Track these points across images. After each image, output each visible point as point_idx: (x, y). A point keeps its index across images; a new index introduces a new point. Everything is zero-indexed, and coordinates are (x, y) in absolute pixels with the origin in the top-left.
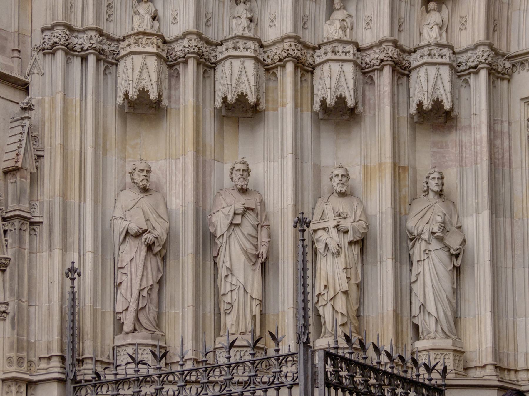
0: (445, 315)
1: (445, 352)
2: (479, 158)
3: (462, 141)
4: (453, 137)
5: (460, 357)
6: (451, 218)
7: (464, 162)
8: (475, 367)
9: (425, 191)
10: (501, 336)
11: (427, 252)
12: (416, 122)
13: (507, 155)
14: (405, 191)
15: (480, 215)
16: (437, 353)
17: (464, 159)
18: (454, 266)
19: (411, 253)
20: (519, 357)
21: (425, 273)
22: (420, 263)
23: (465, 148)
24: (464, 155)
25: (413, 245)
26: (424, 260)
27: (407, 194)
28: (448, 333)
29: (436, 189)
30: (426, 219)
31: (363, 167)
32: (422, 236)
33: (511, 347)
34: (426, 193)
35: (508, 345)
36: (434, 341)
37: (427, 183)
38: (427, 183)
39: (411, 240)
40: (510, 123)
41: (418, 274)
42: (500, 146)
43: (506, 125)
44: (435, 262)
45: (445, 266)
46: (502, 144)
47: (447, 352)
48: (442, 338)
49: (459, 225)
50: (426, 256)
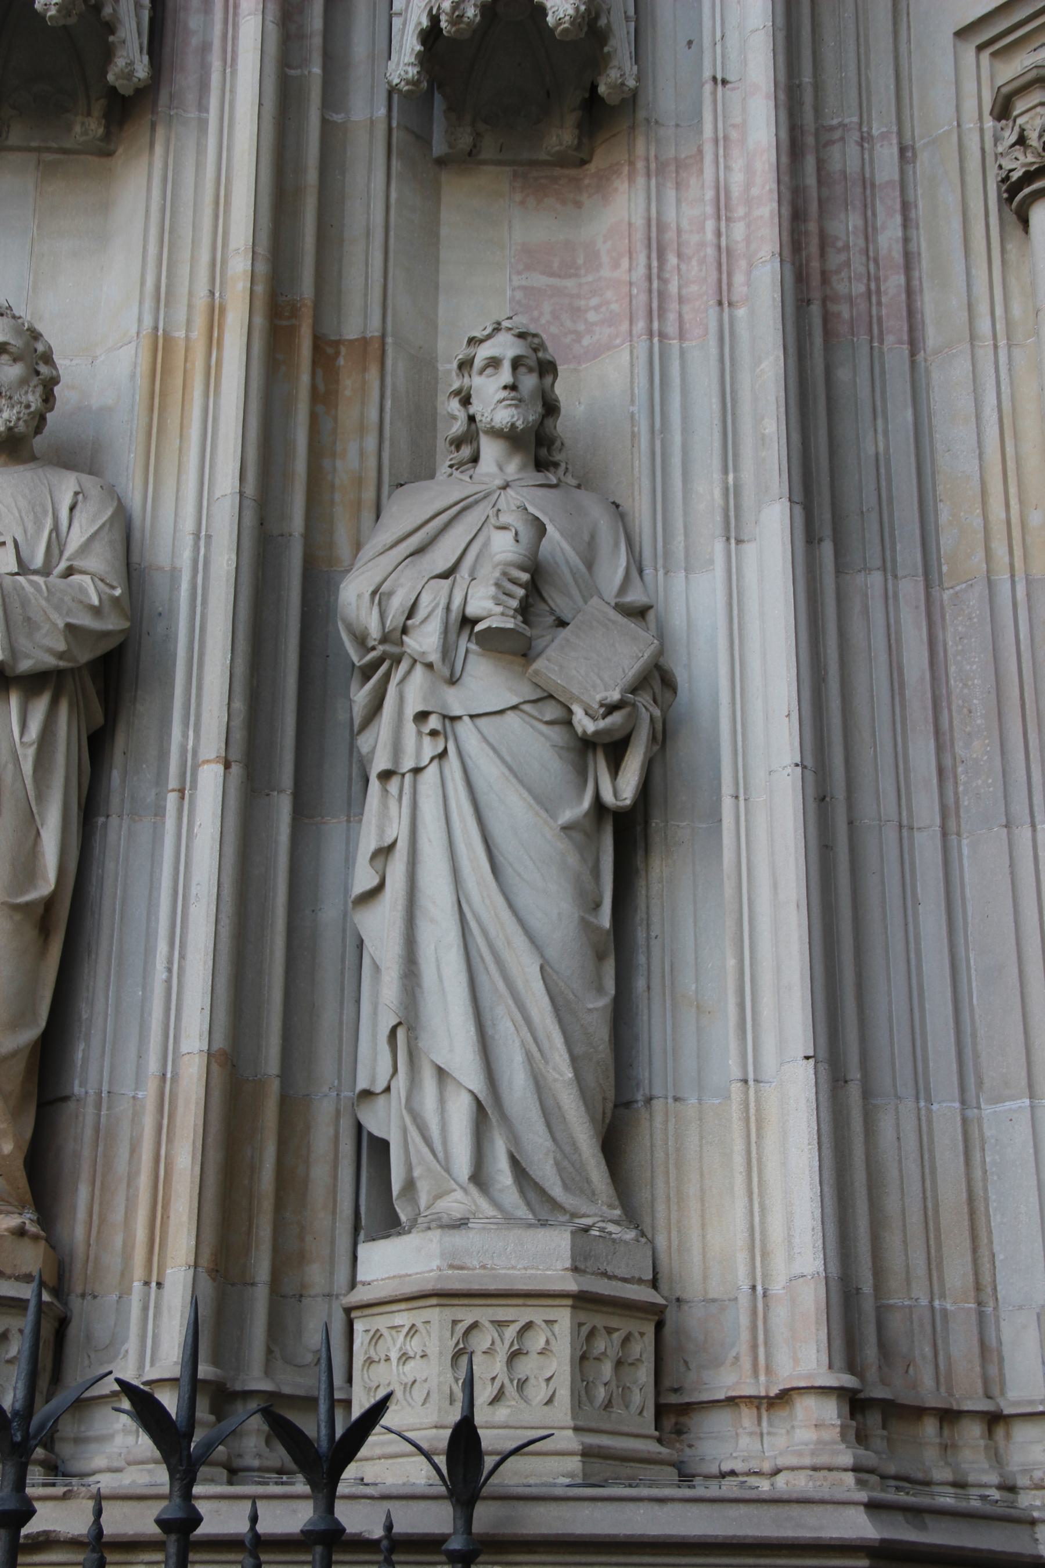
0: (539, 1084)
1: (523, 1314)
2: (739, 278)
3: (661, 228)
4: (621, 208)
5: (627, 1340)
6: (590, 565)
7: (672, 317)
8: (732, 1401)
9: (457, 443)
10: (892, 1204)
11: (433, 722)
12: (441, 162)
13: (894, 283)
14: (362, 453)
15: (750, 549)
16: (468, 1315)
17: (673, 306)
18: (599, 806)
20: (1006, 1335)
22: (395, 782)
23: (679, 256)
24: (673, 288)
26: (417, 771)
27: (372, 462)
28: (557, 1191)
29: (504, 416)
30: (441, 557)
31: (146, 343)
33: (957, 1272)
34: (466, 451)
35: (934, 1264)
36: (458, 1239)
37: (466, 401)
38: (466, 401)
39: (367, 672)
40: (905, 153)
41: (385, 852)
42: (856, 242)
43: (887, 155)
44: (480, 784)
45: (545, 803)
46: (869, 231)
47: (536, 1314)
48: (509, 1220)
49: (635, 596)
50: (430, 748)
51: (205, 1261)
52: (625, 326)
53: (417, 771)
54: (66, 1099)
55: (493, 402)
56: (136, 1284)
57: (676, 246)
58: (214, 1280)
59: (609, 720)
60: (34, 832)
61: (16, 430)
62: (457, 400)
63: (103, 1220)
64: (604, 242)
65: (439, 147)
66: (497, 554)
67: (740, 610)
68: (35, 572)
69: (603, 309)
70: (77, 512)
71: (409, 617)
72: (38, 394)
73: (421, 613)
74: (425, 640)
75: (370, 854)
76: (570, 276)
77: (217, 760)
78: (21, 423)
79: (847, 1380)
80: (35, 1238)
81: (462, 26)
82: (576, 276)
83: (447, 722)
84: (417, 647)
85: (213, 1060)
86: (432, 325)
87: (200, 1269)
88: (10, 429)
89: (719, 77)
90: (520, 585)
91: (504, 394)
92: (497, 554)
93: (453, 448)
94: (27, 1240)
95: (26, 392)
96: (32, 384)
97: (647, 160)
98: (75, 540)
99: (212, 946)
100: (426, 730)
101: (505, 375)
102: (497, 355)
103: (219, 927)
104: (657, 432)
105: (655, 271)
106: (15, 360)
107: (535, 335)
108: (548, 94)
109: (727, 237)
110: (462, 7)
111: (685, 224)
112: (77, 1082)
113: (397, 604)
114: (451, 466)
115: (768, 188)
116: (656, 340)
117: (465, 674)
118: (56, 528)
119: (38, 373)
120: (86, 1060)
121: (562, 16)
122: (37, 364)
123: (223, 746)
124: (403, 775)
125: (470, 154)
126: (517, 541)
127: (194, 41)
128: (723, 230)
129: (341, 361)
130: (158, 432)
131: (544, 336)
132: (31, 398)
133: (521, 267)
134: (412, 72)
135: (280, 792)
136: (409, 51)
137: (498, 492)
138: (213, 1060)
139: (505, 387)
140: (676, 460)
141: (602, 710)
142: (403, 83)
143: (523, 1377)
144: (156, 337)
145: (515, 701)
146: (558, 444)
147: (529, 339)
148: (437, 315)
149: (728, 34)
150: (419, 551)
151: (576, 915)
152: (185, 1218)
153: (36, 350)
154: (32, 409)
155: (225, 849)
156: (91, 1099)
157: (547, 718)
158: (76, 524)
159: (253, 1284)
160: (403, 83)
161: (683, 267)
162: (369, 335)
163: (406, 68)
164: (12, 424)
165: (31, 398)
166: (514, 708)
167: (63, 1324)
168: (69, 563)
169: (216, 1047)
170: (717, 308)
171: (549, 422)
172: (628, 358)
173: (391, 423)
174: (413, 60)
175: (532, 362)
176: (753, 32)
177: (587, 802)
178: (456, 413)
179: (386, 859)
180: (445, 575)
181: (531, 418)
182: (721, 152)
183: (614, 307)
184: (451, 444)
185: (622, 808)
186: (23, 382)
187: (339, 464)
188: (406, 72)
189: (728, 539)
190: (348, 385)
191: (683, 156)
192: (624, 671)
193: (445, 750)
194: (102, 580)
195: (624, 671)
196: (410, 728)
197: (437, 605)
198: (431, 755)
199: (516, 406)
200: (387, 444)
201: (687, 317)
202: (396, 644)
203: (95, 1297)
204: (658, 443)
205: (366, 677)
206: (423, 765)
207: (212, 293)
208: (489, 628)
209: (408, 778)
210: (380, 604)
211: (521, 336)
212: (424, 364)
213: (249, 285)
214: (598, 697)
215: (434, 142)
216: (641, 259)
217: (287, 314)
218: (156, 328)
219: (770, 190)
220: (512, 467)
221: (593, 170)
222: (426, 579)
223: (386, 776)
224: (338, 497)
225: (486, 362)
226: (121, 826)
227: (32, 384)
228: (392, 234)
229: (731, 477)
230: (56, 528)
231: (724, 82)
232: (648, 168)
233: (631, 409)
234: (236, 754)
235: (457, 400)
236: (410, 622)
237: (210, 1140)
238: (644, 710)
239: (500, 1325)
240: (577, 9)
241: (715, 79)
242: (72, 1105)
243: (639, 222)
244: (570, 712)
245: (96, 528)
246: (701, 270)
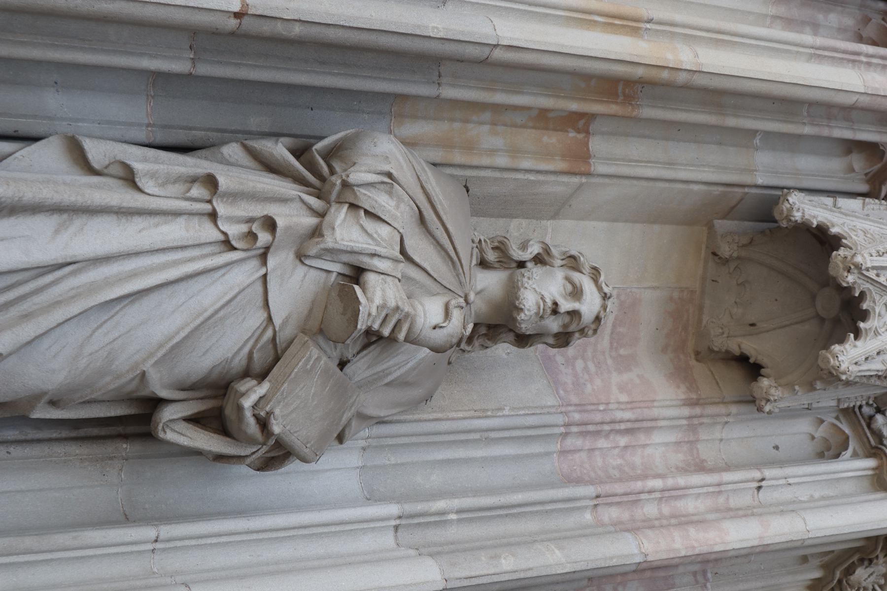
3: (649, 430)
7: (579, 442)
9: (501, 248)
11: (264, 237)
12: (710, 226)
14: (492, 152)
17: (588, 443)
18: (156, 403)
19: (232, 150)
21: (138, 223)
24: (602, 443)
25: (271, 167)
26: (213, 216)
27: (485, 161)
29: (529, 301)
32: (340, 216)
37: (539, 260)
38: (539, 260)
41: (129, 178)
50: (234, 230)
52: (574, 399)
53: (213, 216)
55: (541, 290)
57: (633, 444)
59: (252, 421)
62: (541, 251)
64: (638, 376)
65: (722, 225)
66: (423, 305)
67: (335, 533)
69: (586, 377)
71: (367, 212)
73: (370, 225)
74: (346, 232)
75: (128, 162)
76: (611, 343)
81: (841, 270)
82: (611, 348)
83: (262, 251)
84: (338, 222)
86: (584, 216)
89: (763, 483)
90: (393, 330)
91: (549, 304)
92: (423, 305)
93: (496, 244)
97: (701, 416)
100: (255, 228)
101: (566, 306)
102: (584, 297)
104: (486, 435)
105: (617, 427)
107: (595, 331)
108: (752, 325)
109: (648, 500)
110: (856, 271)
111: (649, 451)
113: (382, 202)
114: (480, 240)
115: (696, 545)
116: (562, 430)
117: (306, 268)
121: (840, 359)
124: (210, 202)
125: (714, 254)
126: (434, 328)
127: (820, 17)
128: (653, 496)
129: (572, 134)
131: (592, 340)
133: (622, 298)
134: (797, 216)
136: (816, 213)
137: (463, 295)
139: (555, 304)
140: (461, 453)
141: (263, 414)
142: (788, 206)
145: (277, 321)
146: (489, 343)
147: (593, 326)
148: (593, 220)
149: (790, 488)
150: (422, 220)
151: (50, 388)
157: (256, 355)
160: (788, 206)
161: (617, 451)
162: (592, 161)
163: (801, 211)
166: (270, 319)
170: (594, 495)
171: (511, 337)
172: (549, 404)
173: (515, 179)
174: (806, 217)
175: (572, 328)
176: (804, 519)
177: (164, 394)
178: (530, 250)
179: (120, 178)
180: (403, 251)
181: (523, 326)
182: (711, 489)
183: (589, 388)
184: (500, 242)
185: (156, 428)
187: (486, 128)
188: (798, 210)
189: (400, 517)
190: (551, 139)
191: (699, 446)
192: (296, 432)
193: (234, 249)
195: (296, 432)
196: (259, 210)
197: (378, 244)
198: (230, 233)
199: (537, 314)
200: (498, 174)
201: (577, 456)
202: (339, 196)
204: (477, 436)
205: (298, 153)
206: (219, 223)
207: (650, 21)
208: (359, 303)
209: (207, 207)
210: (383, 183)
211: (598, 319)
212: (557, 209)
213: (671, 66)
214: (277, 411)
215: (725, 221)
216: (628, 415)
219: (694, 547)
220: (479, 305)
221: (691, 363)
222: (401, 231)
223: (211, 182)
224: (457, 125)
225: (578, 285)
228: (667, 185)
229: (453, 517)
231: (759, 488)
232: (695, 417)
233: (507, 408)
235: (541, 251)
236: (362, 213)
238: (254, 450)
240: (844, 373)
241: (763, 480)
243: (656, 412)
244: (262, 376)
246: (614, 468)
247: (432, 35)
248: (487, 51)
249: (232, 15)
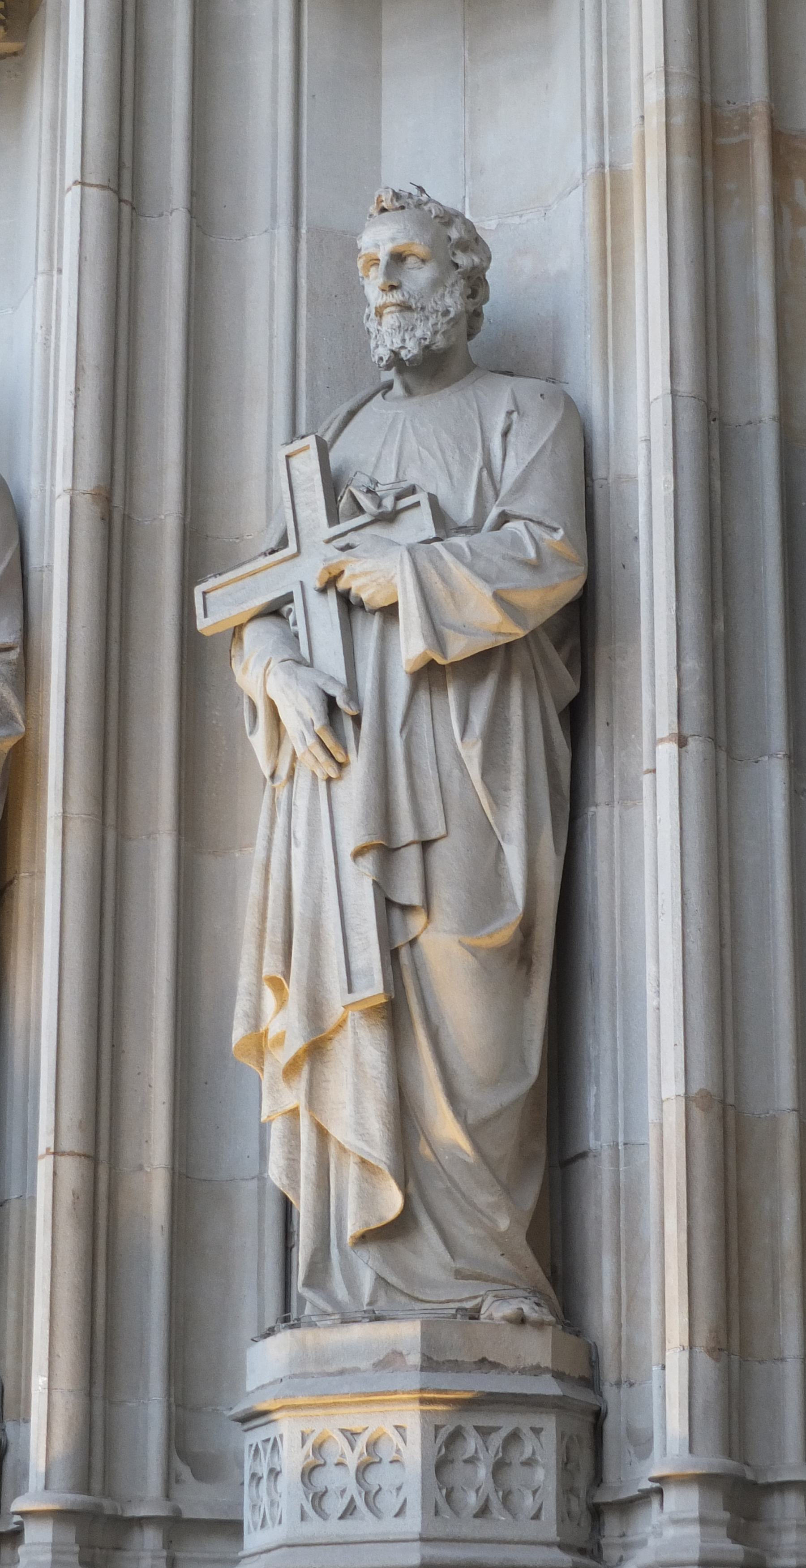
51: (702, 1340)
54: (583, 1155)
56: (654, 1368)
58: (717, 1360)
60: (496, 843)
61: (434, 347)
63: (632, 1296)
68: (462, 530)
70: (511, 438)
72: (457, 294)
77: (669, 739)
78: (439, 337)
79: (731, 1465)
80: (539, 1325)
85: (693, 1105)
87: (697, 1350)
88: (427, 347)
94: (528, 1328)
95: (443, 296)
96: (449, 282)
98: (512, 471)
99: (681, 968)
103: (688, 944)
106: (424, 261)
112: (591, 1135)
118: (487, 464)
119: (457, 266)
120: (597, 1105)
122: (454, 254)
123: (675, 720)
130: (614, 302)
132: (449, 301)
135: (770, 756)
138: (693, 1105)
143: (320, 1489)
144: (603, 175)
152: (676, 1293)
153: (450, 239)
154: (452, 315)
155: (688, 846)
156: (606, 1155)
158: (511, 453)
159: (783, 1360)
164: (427, 343)
165: (449, 301)
167: (598, 1419)
168: (500, 509)
169: (695, 1088)
186: (437, 284)
194: (540, 523)
203: (631, 1385)
217: (736, 128)
218: (602, 165)
226: (611, 816)
227: (449, 282)
230: (487, 464)
234: (692, 725)
237: (698, 1200)
239: (484, 1432)
242: (590, 1161)
245: (534, 454)
247: (672, 489)
248: (682, 403)
249: (684, 749)
